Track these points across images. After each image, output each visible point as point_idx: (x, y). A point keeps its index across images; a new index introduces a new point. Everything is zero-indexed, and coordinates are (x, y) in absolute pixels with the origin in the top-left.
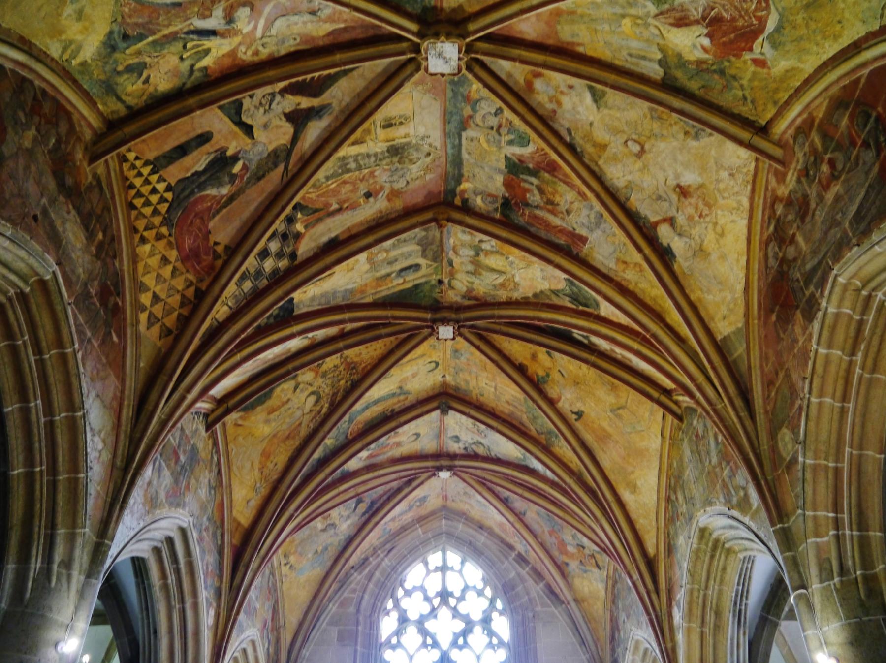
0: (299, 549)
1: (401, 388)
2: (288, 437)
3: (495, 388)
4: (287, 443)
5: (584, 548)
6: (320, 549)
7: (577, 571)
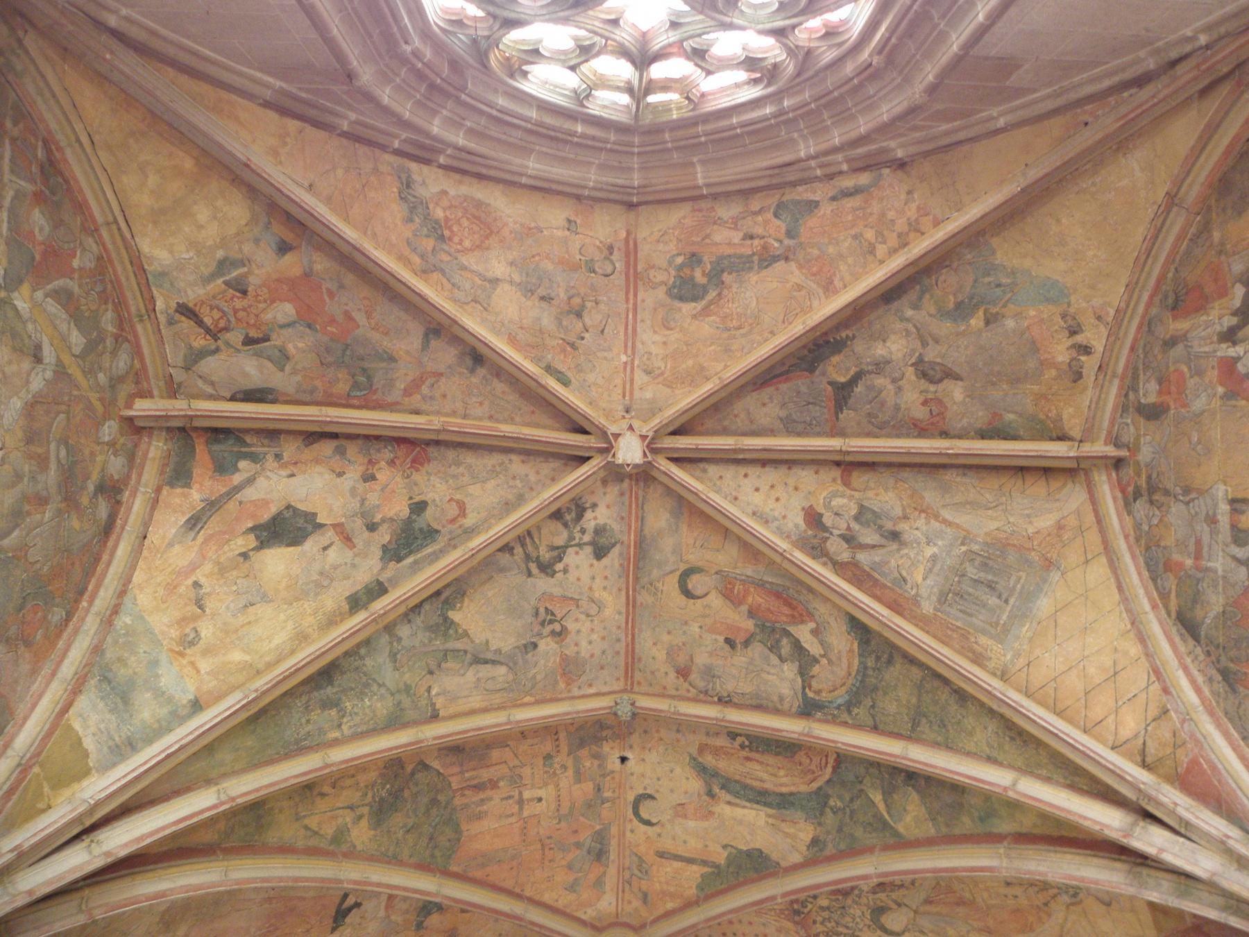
0: (1032, 364)
1: (711, 794)
2: (961, 902)
3: (521, 802)
4: (968, 895)
5: (249, 341)
6: (976, 321)
7: (247, 248)
